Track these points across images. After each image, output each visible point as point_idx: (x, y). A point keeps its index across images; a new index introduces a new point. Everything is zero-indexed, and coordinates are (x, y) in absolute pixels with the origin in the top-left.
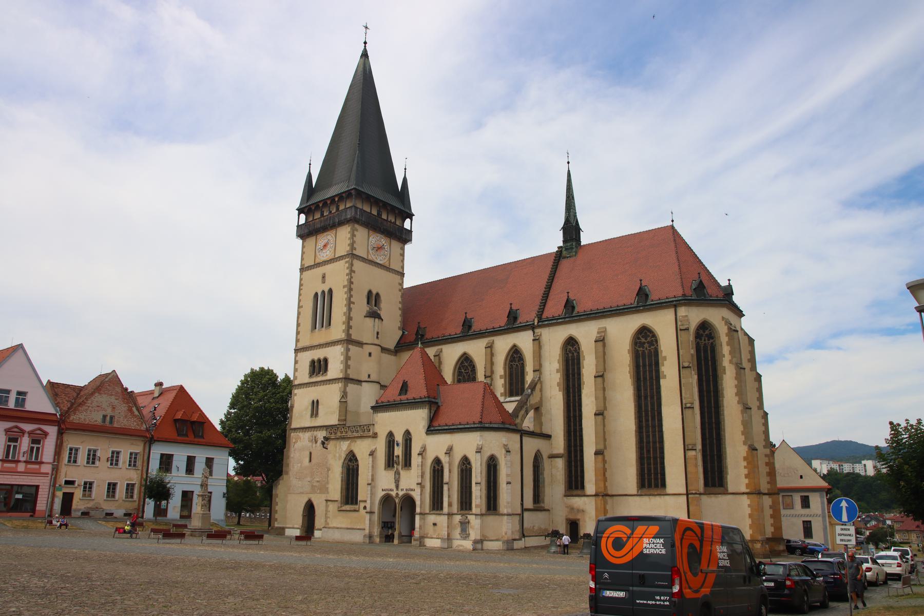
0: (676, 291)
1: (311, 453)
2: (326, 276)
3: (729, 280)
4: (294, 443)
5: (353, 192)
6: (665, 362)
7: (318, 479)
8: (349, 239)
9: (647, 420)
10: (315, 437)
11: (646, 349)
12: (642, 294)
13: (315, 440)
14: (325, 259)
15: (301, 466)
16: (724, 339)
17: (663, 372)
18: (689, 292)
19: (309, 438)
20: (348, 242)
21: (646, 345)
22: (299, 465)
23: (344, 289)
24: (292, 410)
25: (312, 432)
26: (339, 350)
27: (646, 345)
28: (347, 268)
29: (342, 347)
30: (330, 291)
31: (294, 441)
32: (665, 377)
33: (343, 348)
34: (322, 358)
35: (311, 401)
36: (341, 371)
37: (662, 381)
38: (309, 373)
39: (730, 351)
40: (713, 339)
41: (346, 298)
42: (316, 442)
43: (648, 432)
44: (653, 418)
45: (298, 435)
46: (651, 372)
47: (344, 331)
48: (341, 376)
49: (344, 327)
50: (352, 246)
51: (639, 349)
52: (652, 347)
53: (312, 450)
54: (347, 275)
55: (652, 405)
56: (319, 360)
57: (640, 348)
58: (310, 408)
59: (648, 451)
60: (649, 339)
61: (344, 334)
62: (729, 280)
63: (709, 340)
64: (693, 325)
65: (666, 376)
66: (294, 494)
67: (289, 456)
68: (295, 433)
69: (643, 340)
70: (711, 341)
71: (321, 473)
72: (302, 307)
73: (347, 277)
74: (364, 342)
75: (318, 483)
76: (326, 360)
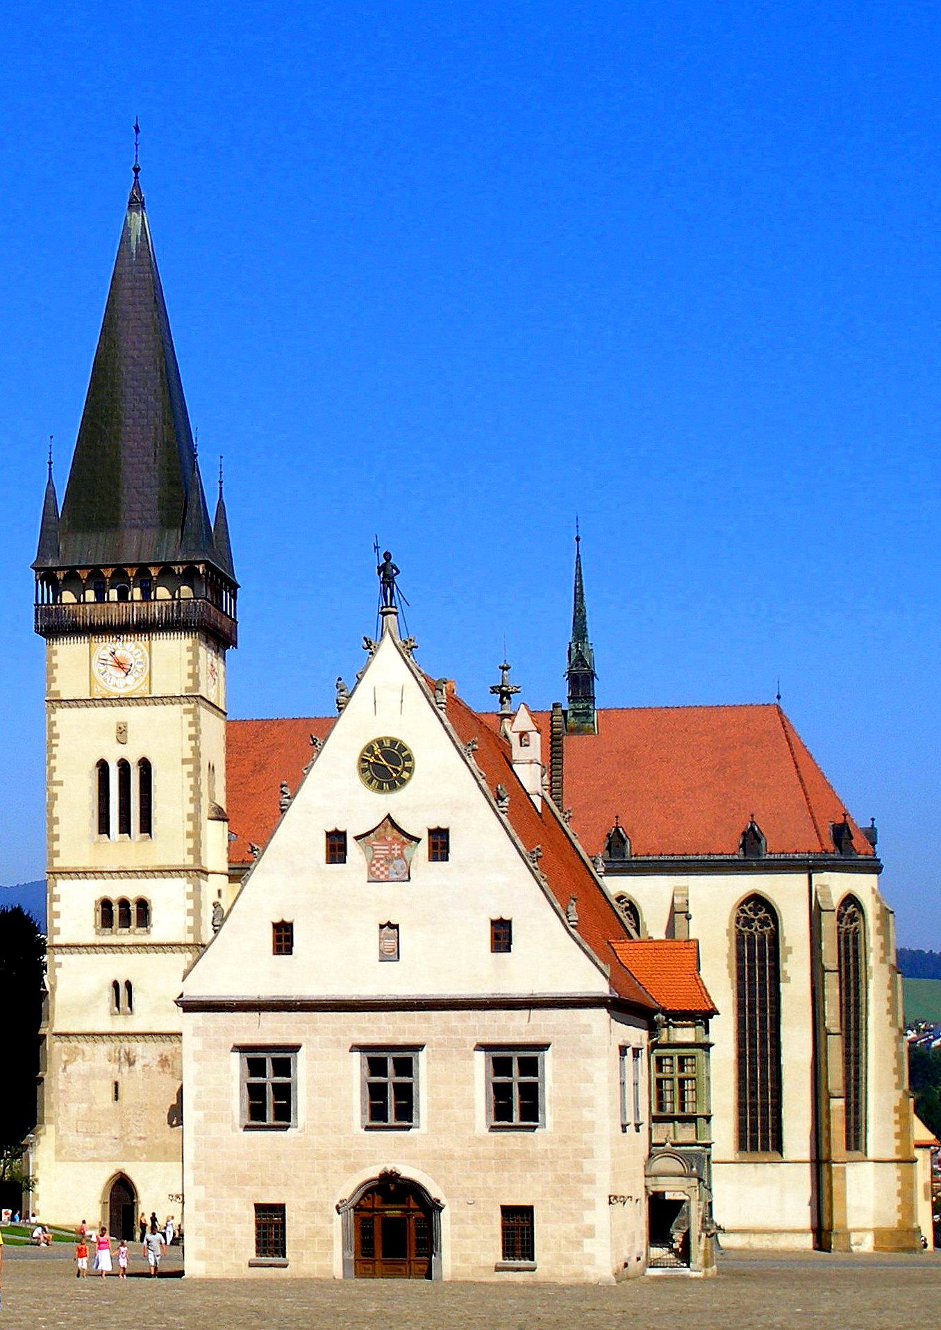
0: (810, 843)
1: (116, 1084)
2: (129, 729)
3: (873, 819)
4: (66, 1061)
5: (201, 568)
6: (789, 957)
7: (138, 1135)
8: (190, 662)
9: (753, 1046)
10: (128, 1054)
11: (756, 930)
12: (751, 839)
13: (129, 1059)
14: (123, 692)
15: (90, 1109)
16: (872, 922)
17: (785, 972)
18: (830, 846)
19: (109, 1054)
20: (190, 669)
21: (756, 924)
22: (85, 1106)
23: (184, 766)
24: (53, 995)
25: (118, 1043)
26: (180, 885)
27: (756, 924)
28: (191, 724)
29: (188, 883)
30: (145, 765)
31: (65, 1057)
32: (788, 980)
33: (191, 886)
34: (132, 897)
35: (111, 984)
36: (190, 930)
37: (782, 985)
38: (95, 926)
39: (882, 944)
40: (856, 921)
41: (191, 786)
42: (131, 1063)
43: (753, 1063)
44: (764, 1042)
45: (76, 1047)
46: (762, 968)
47: (190, 852)
48: (190, 939)
49: (190, 843)
50: (194, 676)
51: (743, 929)
52: (765, 928)
53: (118, 1079)
54: (190, 739)
55: (763, 1020)
56: (124, 903)
57: (744, 927)
58: (108, 994)
59: (753, 1094)
60: (761, 914)
61: (192, 857)
62: (873, 819)
63: (851, 924)
64: (836, 900)
65: (789, 978)
66: (73, 1161)
67: (52, 1088)
68: (67, 1044)
69: (751, 915)
70: (854, 925)
71: (150, 1122)
72: (60, 783)
73: (193, 743)
74: (209, 870)
75: (143, 1142)
76: (143, 904)
